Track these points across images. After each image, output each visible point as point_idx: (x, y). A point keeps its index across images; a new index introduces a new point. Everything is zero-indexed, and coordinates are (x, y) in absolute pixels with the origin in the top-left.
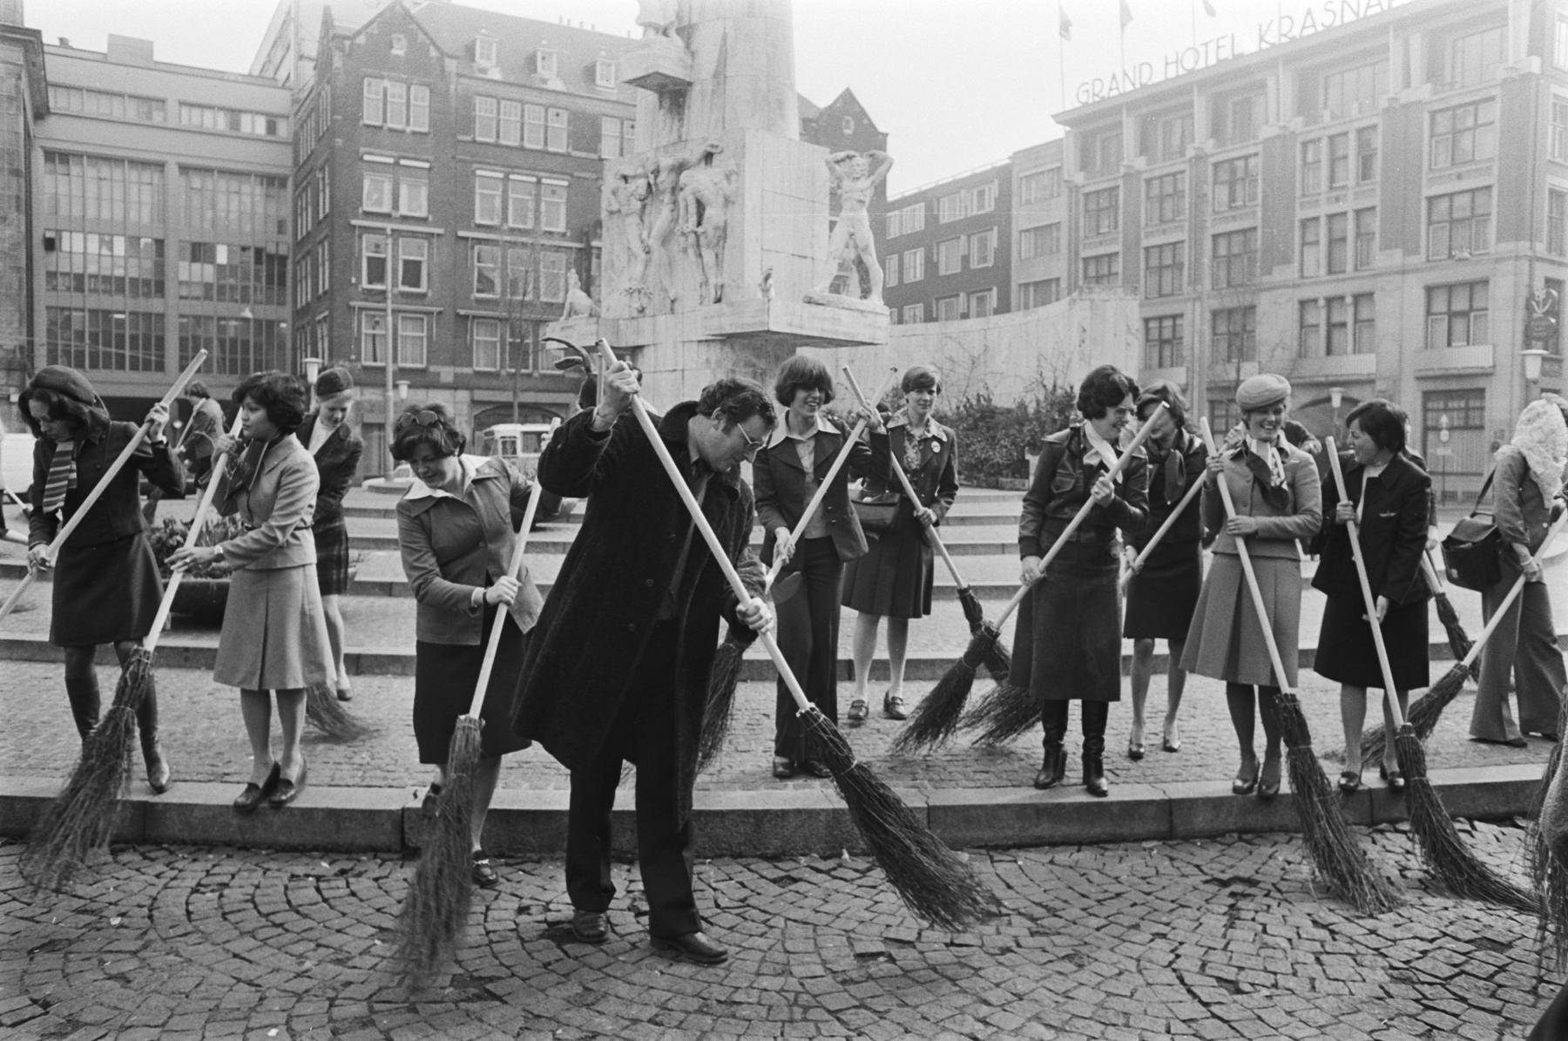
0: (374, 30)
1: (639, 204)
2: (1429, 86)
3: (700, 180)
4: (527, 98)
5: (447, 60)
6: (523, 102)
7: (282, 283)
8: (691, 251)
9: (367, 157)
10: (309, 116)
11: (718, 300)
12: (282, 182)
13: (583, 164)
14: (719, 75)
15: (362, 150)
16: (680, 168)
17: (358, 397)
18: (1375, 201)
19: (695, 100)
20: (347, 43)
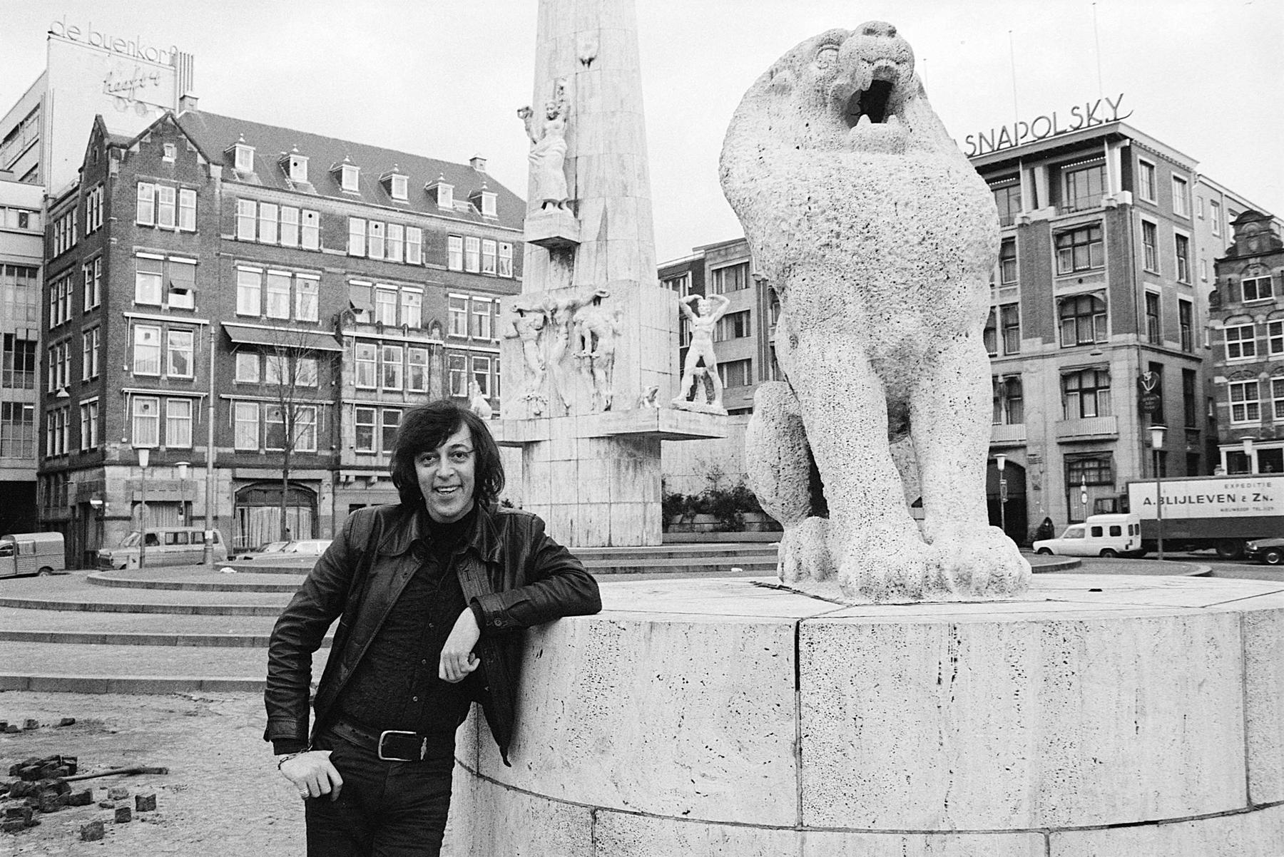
0: (147, 139)
1: (536, 333)
2: (1052, 208)
3: (591, 317)
4: (282, 201)
5: (212, 166)
6: (279, 205)
7: (30, 367)
8: (584, 371)
9: (139, 255)
10: (70, 211)
11: (608, 409)
12: (33, 271)
13: (334, 261)
14: (602, 238)
15: (135, 248)
16: (573, 308)
17: (128, 478)
18: (1016, 298)
19: (582, 256)
20: (123, 151)
